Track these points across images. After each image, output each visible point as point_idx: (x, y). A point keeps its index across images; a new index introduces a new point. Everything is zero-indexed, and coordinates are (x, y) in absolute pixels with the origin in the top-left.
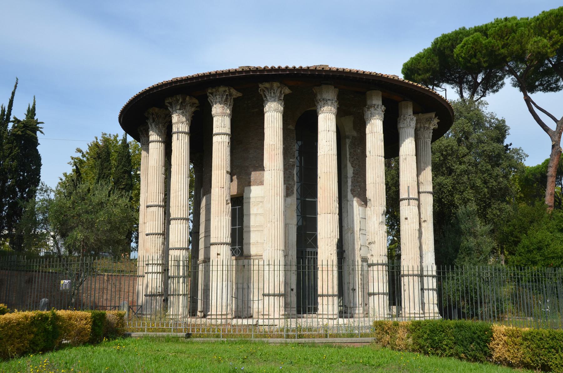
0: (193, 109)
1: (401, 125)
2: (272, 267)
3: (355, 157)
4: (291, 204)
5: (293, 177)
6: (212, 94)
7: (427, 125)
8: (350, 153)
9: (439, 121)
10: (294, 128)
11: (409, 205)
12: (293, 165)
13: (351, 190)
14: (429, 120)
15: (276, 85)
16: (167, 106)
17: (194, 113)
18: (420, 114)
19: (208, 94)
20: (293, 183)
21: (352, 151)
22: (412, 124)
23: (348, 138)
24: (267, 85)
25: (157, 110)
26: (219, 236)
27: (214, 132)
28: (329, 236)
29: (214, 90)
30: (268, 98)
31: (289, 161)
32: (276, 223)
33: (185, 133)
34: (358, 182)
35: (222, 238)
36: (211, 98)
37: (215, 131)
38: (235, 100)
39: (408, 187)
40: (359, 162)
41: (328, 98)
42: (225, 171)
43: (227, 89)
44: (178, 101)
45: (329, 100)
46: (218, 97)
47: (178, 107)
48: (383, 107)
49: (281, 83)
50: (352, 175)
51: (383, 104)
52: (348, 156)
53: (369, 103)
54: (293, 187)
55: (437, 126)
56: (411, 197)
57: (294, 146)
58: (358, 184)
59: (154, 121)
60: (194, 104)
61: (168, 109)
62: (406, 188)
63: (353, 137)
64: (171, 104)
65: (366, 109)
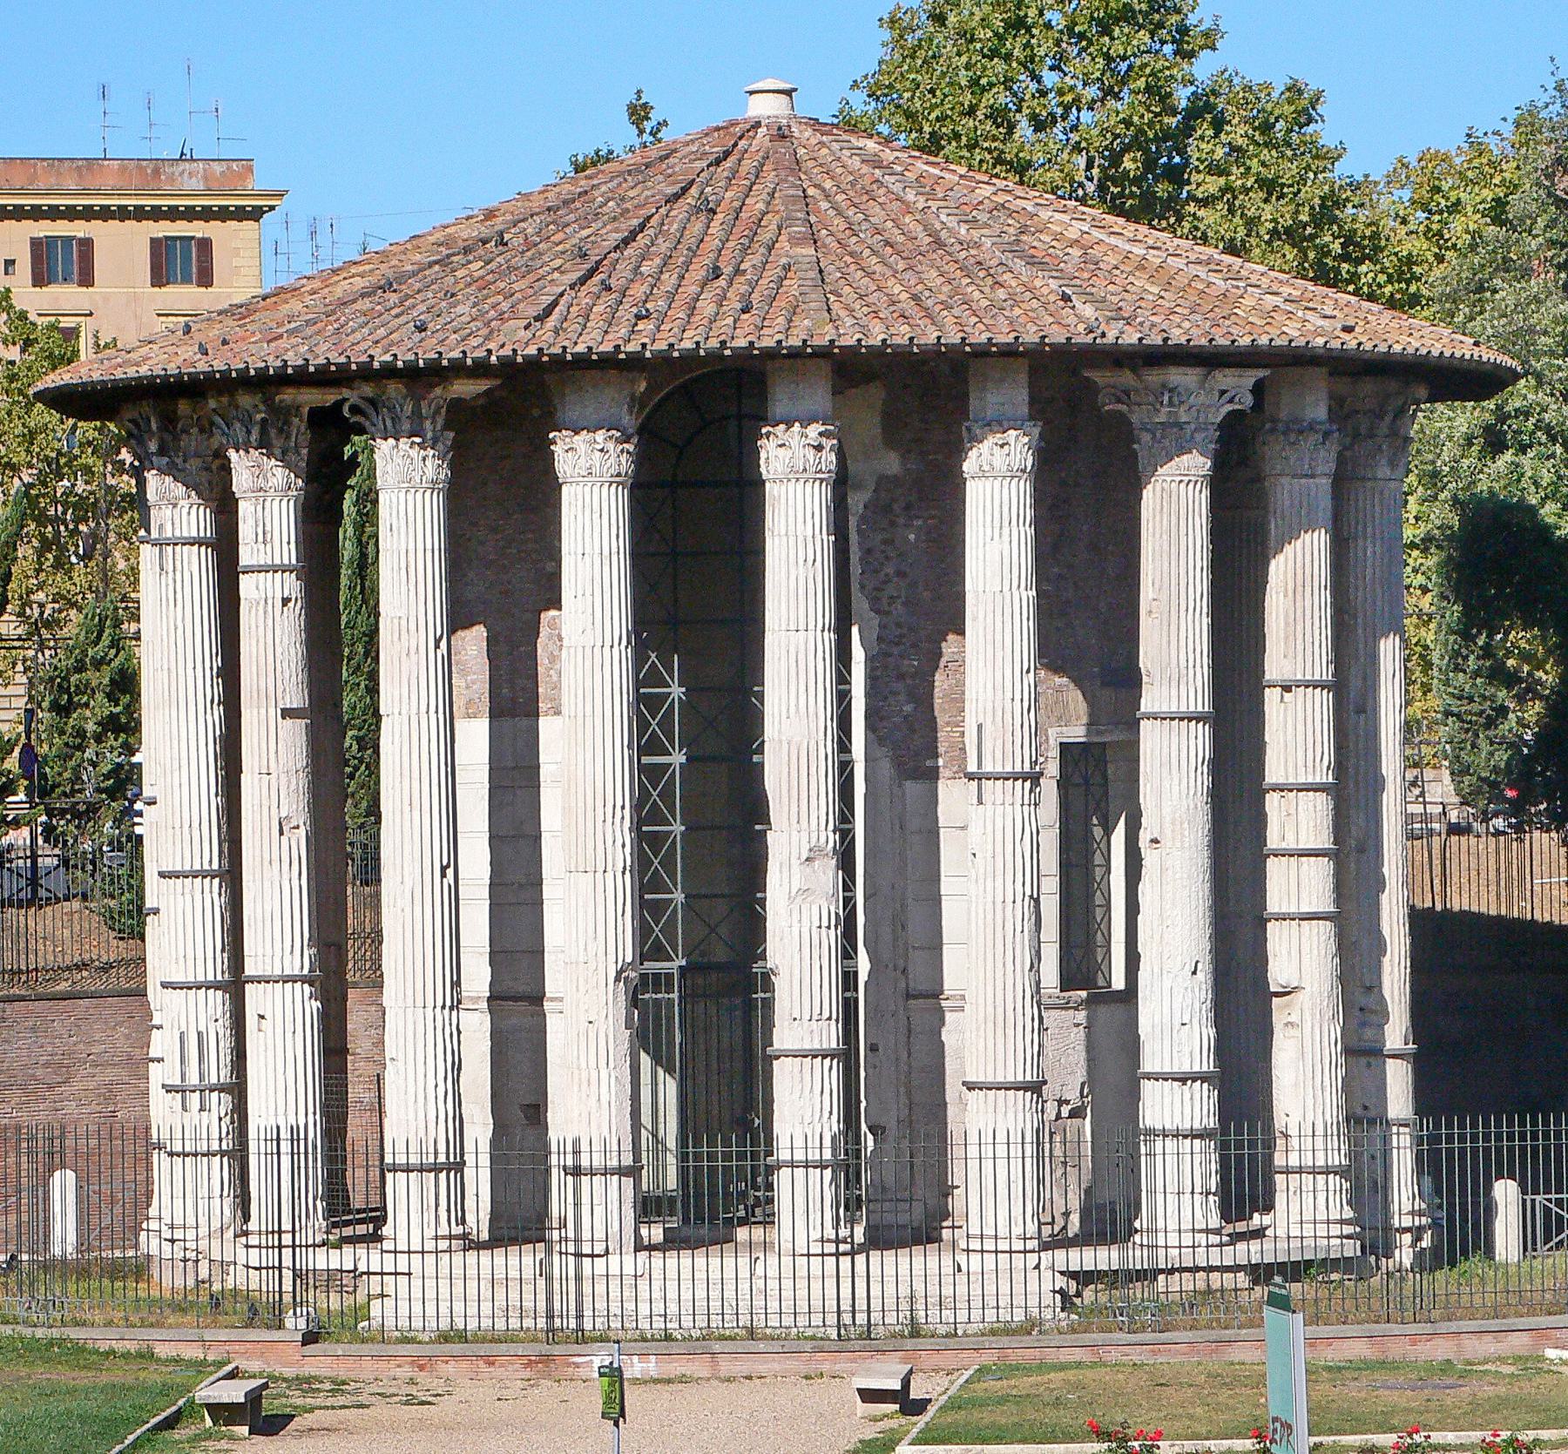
3: (890, 570)
8: (869, 551)
15: (394, 389)
23: (859, 487)
24: (368, 390)
26: (260, 954)
28: (581, 959)
29: (225, 400)
32: (408, 910)
33: (198, 542)
34: (901, 677)
35: (268, 960)
40: (913, 585)
42: (272, 711)
56: (988, 767)
58: (900, 686)
63: (883, 482)
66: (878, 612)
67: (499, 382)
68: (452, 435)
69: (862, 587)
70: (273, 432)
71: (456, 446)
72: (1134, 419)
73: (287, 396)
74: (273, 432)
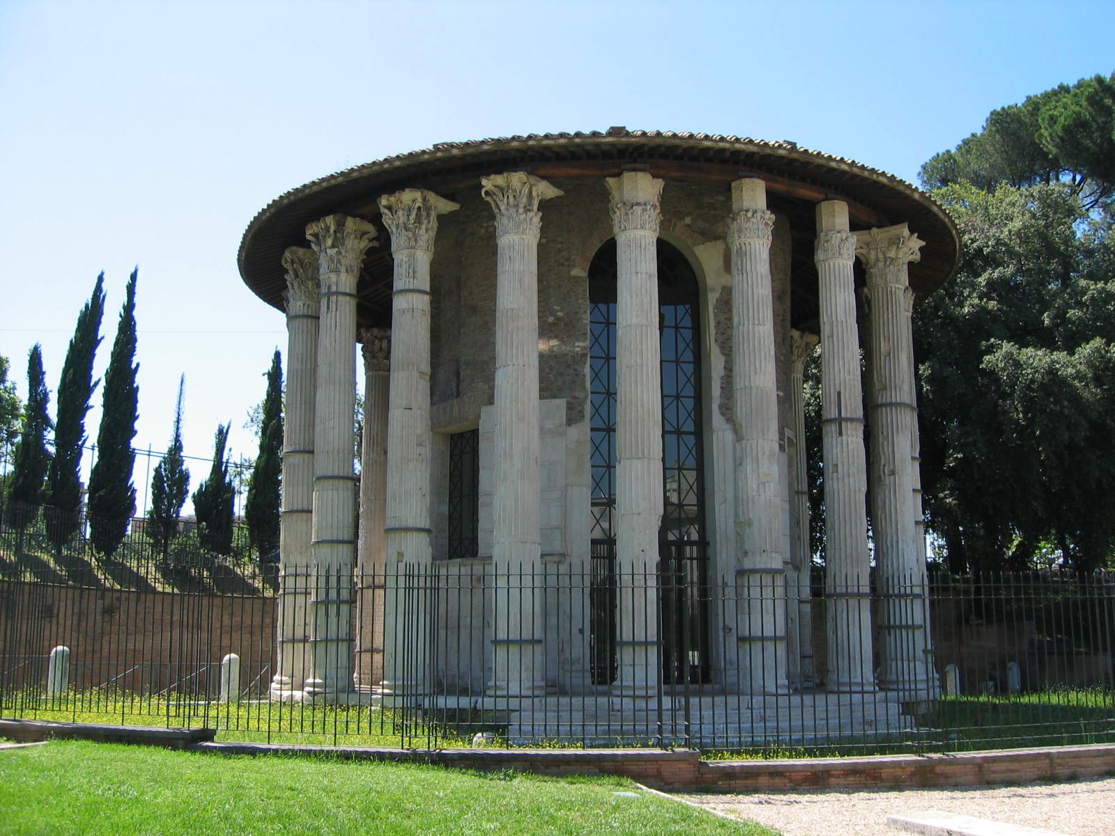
0: (364, 244)
1: (820, 256)
2: (515, 581)
4: (579, 442)
5: (584, 381)
6: (389, 208)
7: (892, 254)
8: (718, 323)
9: (923, 243)
10: (584, 274)
11: (841, 434)
12: (584, 355)
13: (720, 407)
14: (896, 242)
15: (517, 179)
16: (309, 241)
17: (370, 252)
18: (875, 230)
19: (383, 210)
20: (581, 395)
21: (722, 318)
22: (844, 251)
23: (713, 290)
24: (499, 180)
25: (301, 251)
27: (394, 290)
29: (392, 199)
30: (502, 208)
31: (574, 347)
36: (387, 220)
37: (398, 284)
38: (440, 218)
39: (839, 394)
41: (635, 200)
43: (417, 195)
44: (327, 229)
45: (638, 204)
46: (400, 213)
47: (329, 242)
48: (770, 217)
49: (530, 173)
50: (722, 373)
51: (769, 207)
52: (712, 330)
53: (735, 206)
54: (582, 404)
55: (917, 257)
57: (585, 312)
59: (297, 276)
60: (364, 234)
61: (310, 247)
62: (834, 397)
64: (316, 236)
65: (730, 221)
66: (724, 354)
67: (561, 193)
68: (540, 214)
69: (716, 341)
70: (424, 213)
71: (542, 219)
72: (873, 255)
73: (433, 198)
74: (424, 213)
